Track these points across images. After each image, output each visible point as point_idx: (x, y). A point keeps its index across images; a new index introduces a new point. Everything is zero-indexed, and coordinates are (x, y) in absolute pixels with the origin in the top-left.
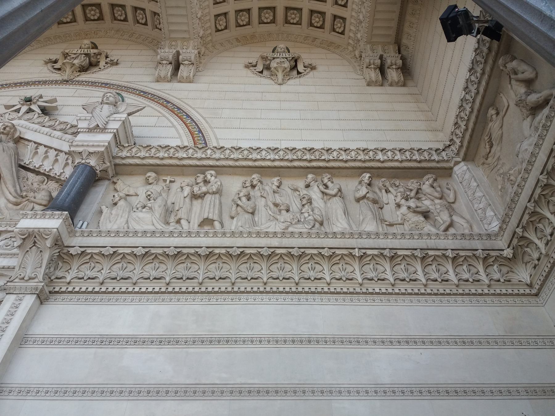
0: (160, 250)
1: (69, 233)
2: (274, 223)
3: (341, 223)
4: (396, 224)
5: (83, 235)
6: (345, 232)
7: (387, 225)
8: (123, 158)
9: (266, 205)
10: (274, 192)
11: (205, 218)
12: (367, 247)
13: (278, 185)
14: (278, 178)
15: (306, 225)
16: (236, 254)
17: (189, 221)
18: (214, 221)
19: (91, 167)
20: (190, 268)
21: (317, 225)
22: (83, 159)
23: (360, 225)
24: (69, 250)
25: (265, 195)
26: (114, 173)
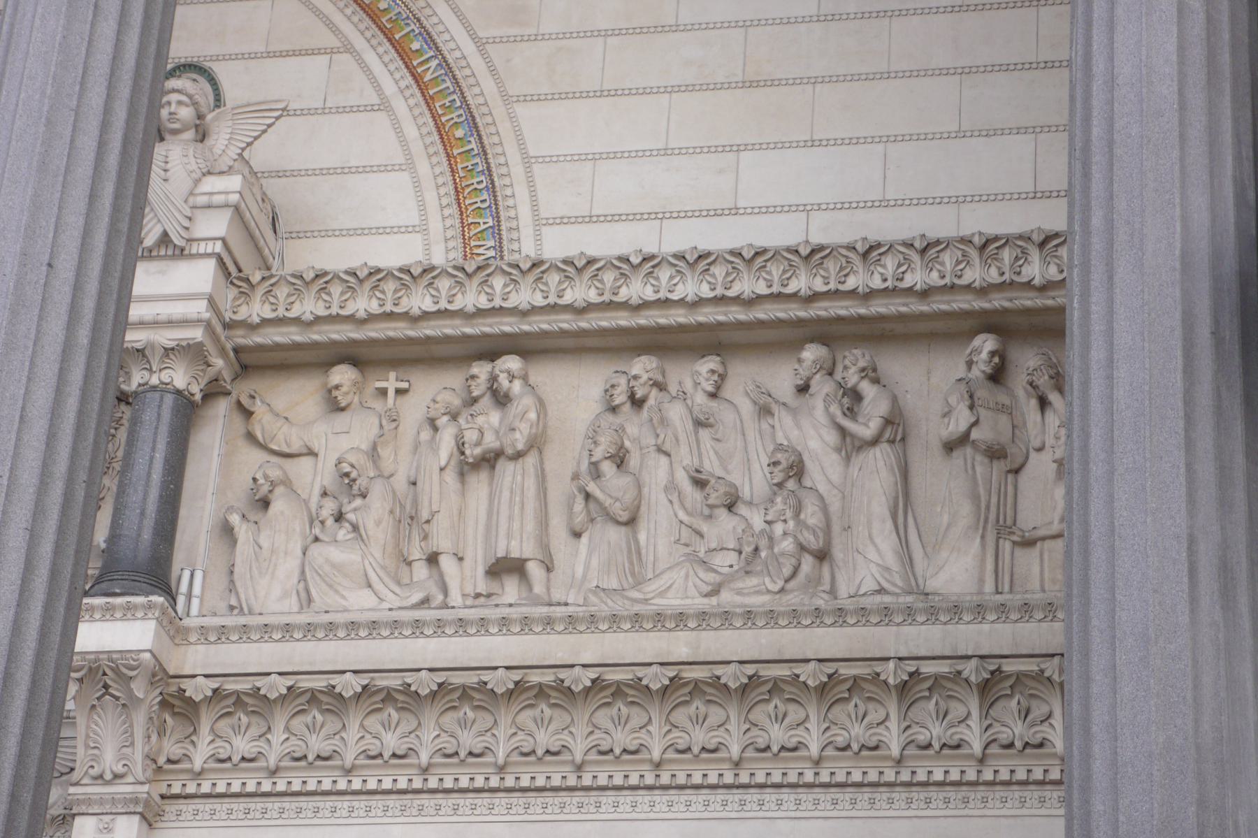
0: (395, 678)
1: (172, 638)
2: (683, 573)
3: (878, 550)
4: (1043, 539)
5: (206, 639)
6: (869, 607)
7: (1014, 543)
8: (253, 328)
9: (671, 487)
10: (699, 424)
11: (499, 555)
12: (923, 653)
13: (710, 389)
14: (712, 366)
15: (767, 580)
16: (581, 687)
17: (460, 555)
18: (526, 560)
19: (178, 392)
20: (474, 721)
21: (808, 563)
22: (150, 370)
23: (937, 547)
24: (183, 687)
25: (667, 447)
26: (237, 366)
